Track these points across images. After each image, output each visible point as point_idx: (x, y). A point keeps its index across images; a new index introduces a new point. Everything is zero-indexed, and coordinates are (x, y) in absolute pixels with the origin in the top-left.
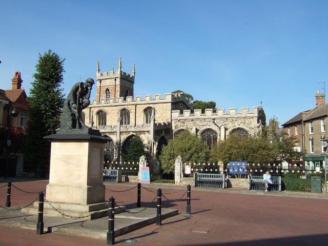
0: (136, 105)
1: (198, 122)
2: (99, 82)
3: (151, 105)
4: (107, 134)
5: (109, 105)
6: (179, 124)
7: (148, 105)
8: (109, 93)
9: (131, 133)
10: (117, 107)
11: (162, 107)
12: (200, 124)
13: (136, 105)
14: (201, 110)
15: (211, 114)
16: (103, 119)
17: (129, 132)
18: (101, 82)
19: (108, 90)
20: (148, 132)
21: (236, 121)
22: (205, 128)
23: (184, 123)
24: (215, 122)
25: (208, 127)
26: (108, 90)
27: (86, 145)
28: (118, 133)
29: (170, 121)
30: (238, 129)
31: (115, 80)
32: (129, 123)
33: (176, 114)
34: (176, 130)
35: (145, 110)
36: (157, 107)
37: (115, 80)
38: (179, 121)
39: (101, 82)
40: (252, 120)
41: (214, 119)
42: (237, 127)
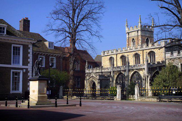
0: (143, 50)
2: (127, 34)
3: (152, 50)
7: (150, 50)
8: (135, 41)
9: (135, 70)
13: (143, 50)
14: (177, 51)
15: (176, 55)
18: (129, 34)
19: (133, 39)
20: (144, 69)
23: (174, 61)
26: (133, 39)
27: (37, 82)
29: (164, 59)
31: (138, 32)
32: (140, 64)
33: (168, 55)
35: (149, 53)
37: (138, 32)
38: (171, 59)
39: (129, 34)
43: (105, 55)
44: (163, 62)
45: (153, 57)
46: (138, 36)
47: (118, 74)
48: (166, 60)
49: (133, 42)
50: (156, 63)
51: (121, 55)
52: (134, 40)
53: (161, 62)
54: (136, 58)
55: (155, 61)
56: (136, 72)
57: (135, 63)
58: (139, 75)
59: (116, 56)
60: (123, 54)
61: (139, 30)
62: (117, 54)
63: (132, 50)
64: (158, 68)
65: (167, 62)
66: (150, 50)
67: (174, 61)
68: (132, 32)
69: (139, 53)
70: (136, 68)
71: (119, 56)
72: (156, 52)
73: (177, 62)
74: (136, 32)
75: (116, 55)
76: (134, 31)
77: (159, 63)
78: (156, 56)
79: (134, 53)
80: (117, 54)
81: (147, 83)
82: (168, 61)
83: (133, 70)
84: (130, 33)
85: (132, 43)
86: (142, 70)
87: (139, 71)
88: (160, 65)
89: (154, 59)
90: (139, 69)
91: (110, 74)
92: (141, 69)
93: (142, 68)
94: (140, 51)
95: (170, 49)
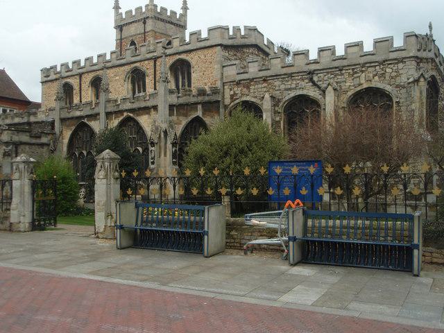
0: (155, 59)
1: (277, 83)
3: (183, 56)
4: (85, 121)
6: (238, 90)
7: (178, 57)
9: (125, 114)
10: (122, 68)
11: (202, 57)
12: (283, 87)
17: (121, 112)
20: (155, 108)
21: (362, 72)
22: (293, 94)
23: (248, 88)
24: (315, 79)
25: (300, 92)
26: (133, 43)
28: (103, 116)
29: (219, 84)
30: (369, 90)
31: (145, 23)
34: (232, 104)
36: (192, 58)
38: (238, 83)
40: (401, 65)
41: (311, 73)
42: (365, 86)
43: (49, 78)
45: (183, 78)
46: (145, 32)
47: (73, 128)
48: (224, 84)
50: (194, 92)
51: (91, 76)
52: (135, 44)
53: (209, 92)
54: (133, 83)
55: (190, 85)
56: (129, 119)
58: (140, 129)
60: (98, 73)
61: (147, 18)
62: (81, 75)
64: (200, 107)
65: (228, 93)
66: (178, 57)
67: (248, 88)
68: (131, 23)
69: (144, 69)
70: (128, 106)
71: (88, 79)
72: (193, 63)
73: (260, 90)
75: (78, 77)
77: (202, 92)
78: (193, 75)
79: (128, 68)
80: (81, 75)
81: (165, 155)
82: (231, 90)
84: (124, 28)
86: (149, 113)
87: (138, 115)
88: (207, 99)
90: (140, 109)
91: (53, 128)
92: (146, 110)
93: (149, 104)
94: (146, 62)
95: (235, 55)
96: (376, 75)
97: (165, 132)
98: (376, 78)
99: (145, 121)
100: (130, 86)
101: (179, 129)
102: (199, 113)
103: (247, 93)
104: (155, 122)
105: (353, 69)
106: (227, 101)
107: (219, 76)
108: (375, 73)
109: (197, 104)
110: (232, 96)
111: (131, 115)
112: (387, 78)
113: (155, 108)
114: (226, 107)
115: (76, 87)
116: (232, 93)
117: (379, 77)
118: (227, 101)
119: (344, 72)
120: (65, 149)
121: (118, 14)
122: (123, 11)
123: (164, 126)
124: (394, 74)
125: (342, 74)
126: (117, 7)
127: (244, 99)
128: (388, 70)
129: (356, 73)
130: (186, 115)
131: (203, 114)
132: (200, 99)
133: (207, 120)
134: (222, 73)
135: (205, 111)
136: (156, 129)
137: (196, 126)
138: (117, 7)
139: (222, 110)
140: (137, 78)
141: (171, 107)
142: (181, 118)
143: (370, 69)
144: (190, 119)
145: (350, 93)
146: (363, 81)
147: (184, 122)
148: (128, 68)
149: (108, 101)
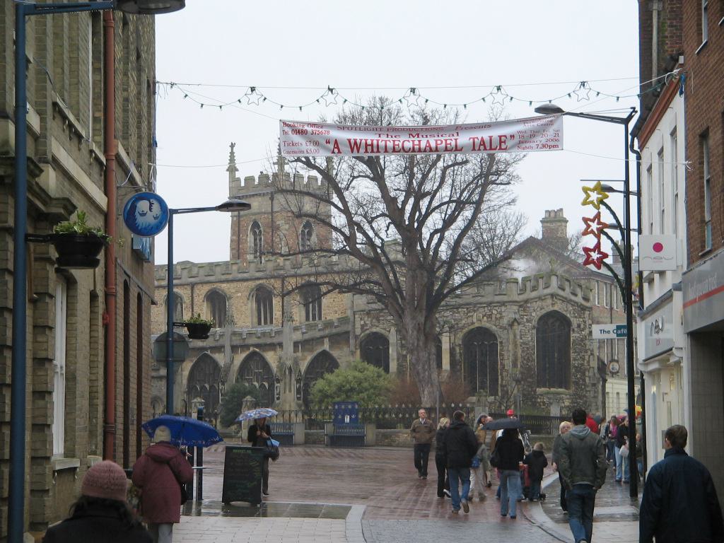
4: (209, 353)
5: (230, 277)
8: (260, 232)
9: (251, 349)
10: (245, 284)
16: (220, 311)
17: (247, 347)
19: (256, 225)
21: (475, 311)
28: (228, 349)
29: (349, 313)
30: (479, 328)
31: (272, 199)
32: (271, 322)
34: (363, 334)
40: (503, 309)
42: (477, 325)
44: (344, 320)
46: (272, 212)
47: (195, 360)
48: (354, 313)
49: (255, 233)
51: (205, 289)
52: (258, 227)
54: (258, 302)
56: (254, 353)
57: (255, 320)
58: (266, 365)
59: (190, 292)
62: (193, 286)
63: (245, 275)
64: (326, 340)
70: (254, 340)
71: (202, 291)
74: (267, 198)
76: (260, 195)
77: (329, 324)
79: (252, 284)
80: (193, 286)
81: (290, 391)
82: (361, 319)
83: (246, 347)
85: (253, 237)
86: (274, 350)
87: (264, 351)
88: (334, 331)
89: (317, 309)
92: (272, 347)
93: (275, 340)
96: (485, 316)
97: (290, 369)
98: (485, 318)
99: (271, 357)
100: (254, 305)
101: (303, 366)
102: (326, 347)
103: (377, 324)
104: (280, 358)
105: (467, 309)
106: (358, 331)
107: (349, 305)
108: (484, 313)
109: (323, 337)
110: (362, 326)
111: (257, 350)
112: (493, 319)
113: (281, 345)
114: (356, 337)
115: (187, 300)
116: (362, 322)
117: (487, 318)
118: (358, 331)
119: (460, 310)
120: (185, 382)
121: (234, 180)
122: (241, 175)
123: (289, 363)
124: (498, 316)
125: (459, 312)
126: (232, 169)
127: (374, 330)
128: (494, 312)
129: (469, 312)
130: (311, 351)
131: (331, 347)
132: (327, 332)
133: (335, 353)
134: (353, 302)
135: (332, 345)
136: (281, 365)
137: (324, 363)
138: (232, 169)
139: (352, 341)
140: (263, 298)
141: (296, 344)
142: (306, 354)
143: (481, 310)
144: (315, 353)
145: (465, 330)
146: (475, 320)
147: (309, 358)
148: (252, 284)
149: (234, 334)
